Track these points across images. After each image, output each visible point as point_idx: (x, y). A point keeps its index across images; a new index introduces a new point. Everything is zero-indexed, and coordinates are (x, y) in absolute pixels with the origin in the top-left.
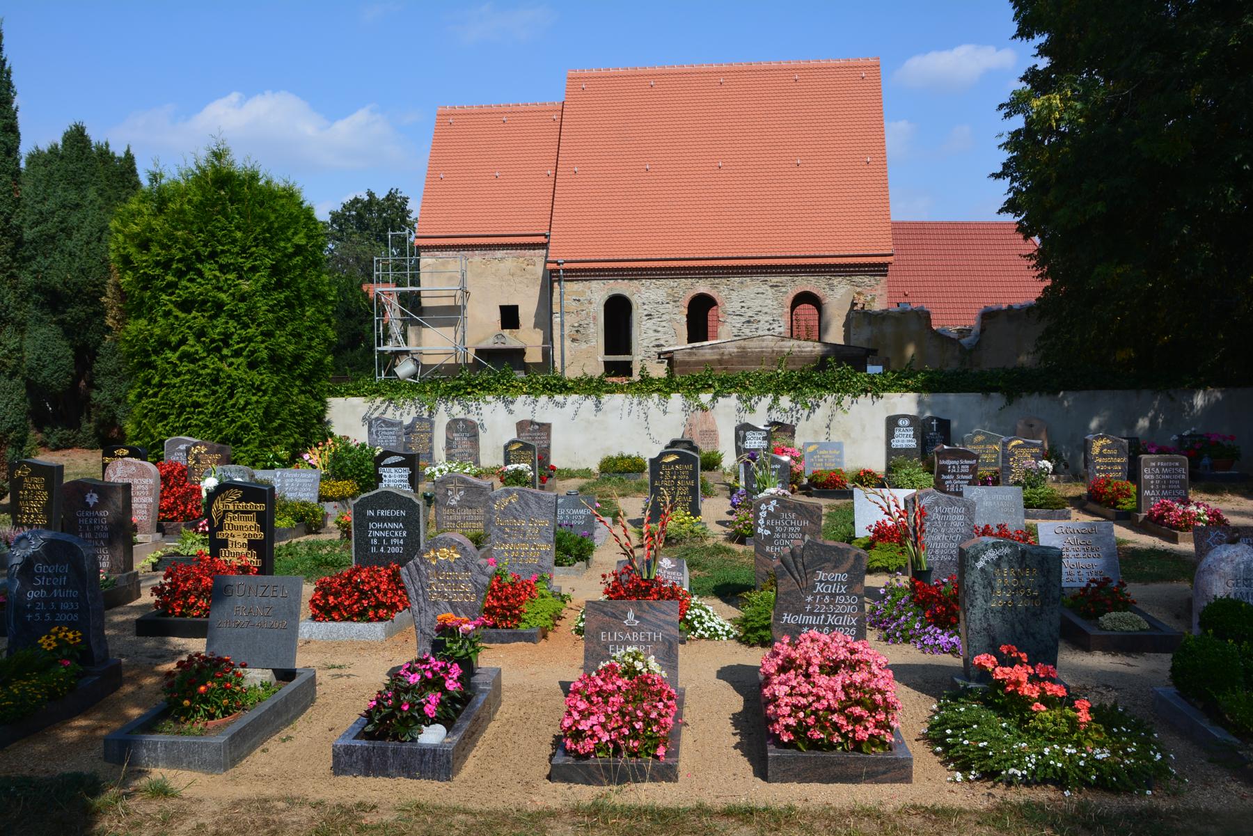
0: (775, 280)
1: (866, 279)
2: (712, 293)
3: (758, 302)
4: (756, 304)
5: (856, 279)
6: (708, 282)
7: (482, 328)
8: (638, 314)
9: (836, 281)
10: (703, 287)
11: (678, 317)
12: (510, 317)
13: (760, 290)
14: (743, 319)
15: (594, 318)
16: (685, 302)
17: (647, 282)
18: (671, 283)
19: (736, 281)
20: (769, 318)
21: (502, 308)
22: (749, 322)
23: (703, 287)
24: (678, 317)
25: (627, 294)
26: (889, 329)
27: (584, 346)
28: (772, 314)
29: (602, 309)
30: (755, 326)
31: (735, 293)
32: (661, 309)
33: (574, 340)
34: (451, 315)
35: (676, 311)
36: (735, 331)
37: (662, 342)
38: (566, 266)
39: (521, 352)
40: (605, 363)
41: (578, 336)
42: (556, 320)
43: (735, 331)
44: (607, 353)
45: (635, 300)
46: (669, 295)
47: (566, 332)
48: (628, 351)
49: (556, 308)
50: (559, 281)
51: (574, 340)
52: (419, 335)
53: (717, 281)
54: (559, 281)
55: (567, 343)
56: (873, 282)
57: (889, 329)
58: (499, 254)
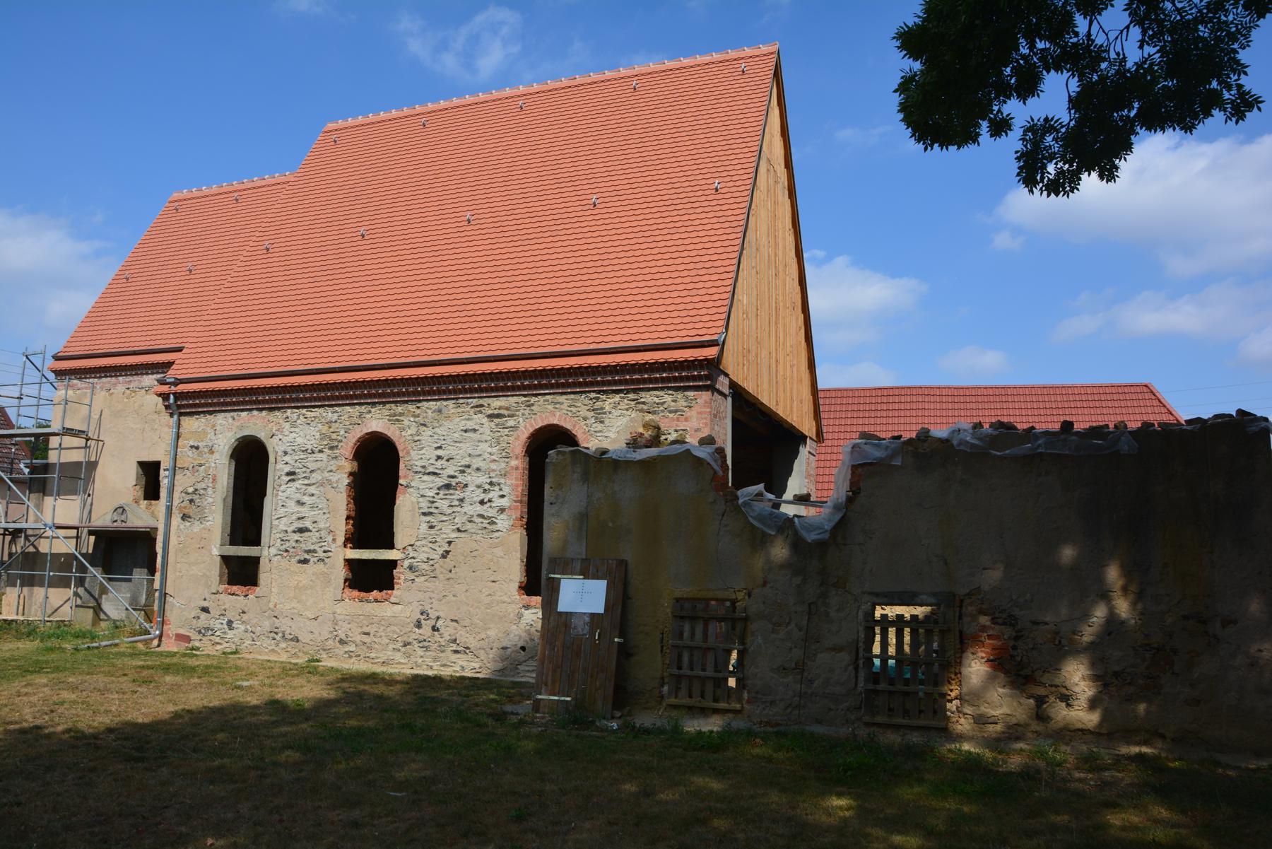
0: (497, 403)
1: (667, 398)
2: (391, 432)
3: (466, 448)
4: (460, 453)
5: (649, 397)
6: (386, 410)
7: (113, 497)
8: (276, 471)
9: (608, 402)
10: (376, 420)
11: (334, 477)
13: (470, 425)
14: (440, 482)
16: (347, 448)
18: (329, 414)
19: (429, 407)
20: (483, 479)
21: (141, 464)
22: (448, 486)
23: (376, 420)
24: (334, 477)
25: (262, 436)
26: (627, 490)
27: (197, 527)
30: (458, 494)
31: (427, 432)
33: (185, 517)
35: (333, 465)
36: (424, 504)
37: (308, 524)
38: (181, 388)
41: (191, 511)
43: (424, 504)
45: (274, 447)
46: (324, 436)
47: (176, 503)
48: (256, 541)
51: (185, 517)
53: (400, 409)
55: (176, 520)
56: (682, 403)
57: (627, 490)
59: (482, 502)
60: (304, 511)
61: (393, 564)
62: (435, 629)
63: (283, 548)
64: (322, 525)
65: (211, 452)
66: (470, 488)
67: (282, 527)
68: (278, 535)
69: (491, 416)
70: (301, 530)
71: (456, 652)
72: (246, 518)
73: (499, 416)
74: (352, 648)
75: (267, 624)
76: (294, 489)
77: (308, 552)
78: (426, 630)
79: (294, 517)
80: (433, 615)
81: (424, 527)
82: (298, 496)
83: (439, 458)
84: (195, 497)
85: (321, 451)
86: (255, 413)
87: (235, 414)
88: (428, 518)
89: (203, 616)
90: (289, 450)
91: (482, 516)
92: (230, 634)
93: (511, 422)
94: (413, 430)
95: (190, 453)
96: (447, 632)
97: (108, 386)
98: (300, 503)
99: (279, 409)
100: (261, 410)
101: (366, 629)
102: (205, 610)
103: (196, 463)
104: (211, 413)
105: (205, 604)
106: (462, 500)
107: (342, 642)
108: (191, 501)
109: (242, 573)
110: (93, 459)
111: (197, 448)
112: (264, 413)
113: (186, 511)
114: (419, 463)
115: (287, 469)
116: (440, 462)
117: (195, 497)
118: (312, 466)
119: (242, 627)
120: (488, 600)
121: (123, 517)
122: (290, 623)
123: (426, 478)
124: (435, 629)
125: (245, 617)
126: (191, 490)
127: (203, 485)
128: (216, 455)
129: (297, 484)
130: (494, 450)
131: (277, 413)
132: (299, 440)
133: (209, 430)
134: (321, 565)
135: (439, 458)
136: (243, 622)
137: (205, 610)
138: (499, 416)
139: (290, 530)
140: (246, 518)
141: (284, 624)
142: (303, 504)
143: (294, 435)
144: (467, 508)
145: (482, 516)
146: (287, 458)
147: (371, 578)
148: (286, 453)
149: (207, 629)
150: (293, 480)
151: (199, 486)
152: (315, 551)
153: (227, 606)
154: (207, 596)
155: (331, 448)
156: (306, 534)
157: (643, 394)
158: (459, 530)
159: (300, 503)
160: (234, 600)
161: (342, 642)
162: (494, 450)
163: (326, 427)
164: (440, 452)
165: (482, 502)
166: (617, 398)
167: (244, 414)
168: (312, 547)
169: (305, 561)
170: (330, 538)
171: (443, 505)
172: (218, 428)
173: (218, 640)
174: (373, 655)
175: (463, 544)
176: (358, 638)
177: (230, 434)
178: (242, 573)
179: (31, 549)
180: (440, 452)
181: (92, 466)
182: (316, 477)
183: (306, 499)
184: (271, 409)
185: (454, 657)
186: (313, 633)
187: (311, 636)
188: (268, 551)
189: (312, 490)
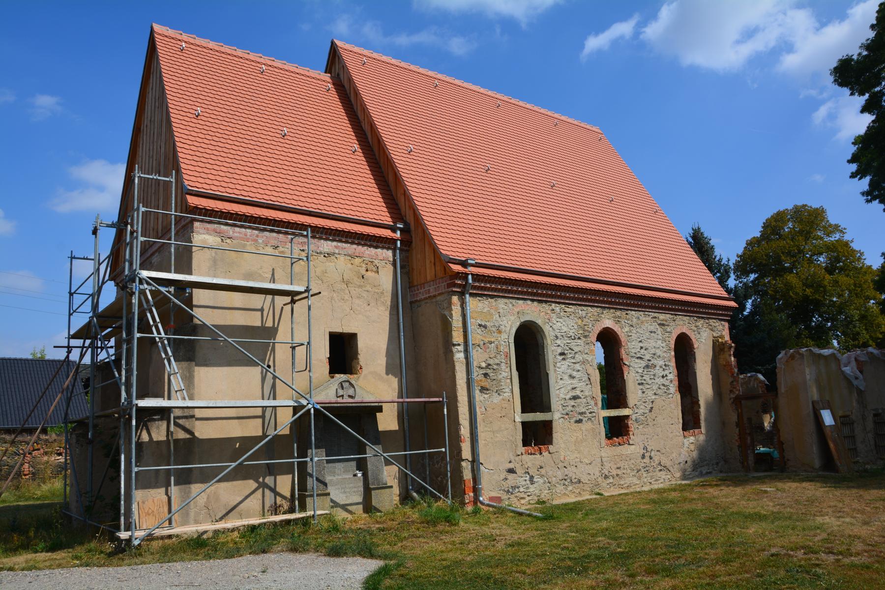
2: (616, 328)
8: (552, 351)
9: (700, 323)
10: (608, 321)
12: (343, 353)
15: (507, 356)
17: (557, 308)
18: (581, 311)
20: (661, 363)
23: (608, 321)
25: (539, 322)
27: (496, 399)
28: (664, 358)
29: (512, 340)
30: (653, 371)
32: (573, 344)
33: (483, 389)
34: (251, 346)
37: (578, 393)
39: (371, 411)
40: (524, 424)
42: (459, 356)
44: (524, 411)
48: (547, 408)
49: (457, 337)
50: (462, 295)
52: (189, 380)
53: (618, 313)
54: (462, 295)
56: (721, 327)
58: (327, 246)
59: (663, 377)
60: (575, 381)
61: (627, 417)
62: (651, 458)
63: (564, 412)
64: (587, 393)
65: (500, 332)
66: (658, 368)
67: (562, 396)
68: (560, 402)
69: (659, 324)
70: (575, 398)
71: (661, 470)
72: (534, 390)
73: (663, 325)
74: (611, 480)
75: (560, 474)
76: (566, 366)
77: (581, 414)
78: (647, 460)
79: (569, 388)
80: (649, 450)
81: (640, 392)
82: (570, 371)
83: (642, 348)
84: (488, 371)
85: (579, 338)
86: (529, 302)
87: (514, 301)
88: (641, 387)
89: (511, 476)
90: (559, 335)
91: (663, 385)
92: (532, 489)
93: (669, 330)
94: (627, 329)
95: (479, 331)
96: (656, 459)
97: (274, 242)
98: (572, 377)
99: (546, 302)
100: (533, 300)
101: (618, 465)
102: (511, 471)
103: (486, 340)
104: (492, 297)
105: (511, 466)
106: (654, 375)
107: (606, 477)
108: (486, 375)
109: (537, 435)
110: (269, 324)
111: (485, 327)
112: (536, 303)
113: (483, 384)
114: (633, 351)
115: (559, 350)
116: (642, 351)
117: (488, 371)
118: (576, 349)
119: (541, 481)
120: (671, 435)
121: (351, 392)
122: (574, 468)
123: (637, 360)
124: (651, 458)
125: (543, 471)
126: (484, 365)
127: (497, 361)
128: (504, 336)
129: (566, 363)
130: (664, 345)
131: (544, 305)
132: (565, 329)
133: (492, 311)
134: (590, 423)
135: (642, 348)
136: (542, 476)
137: (511, 471)
138: (663, 325)
139: (568, 397)
140: (534, 390)
141: (571, 472)
142: (574, 377)
143: (559, 324)
144: (657, 380)
145: (663, 385)
146: (558, 342)
147: (617, 429)
148: (557, 337)
149: (514, 488)
150: (564, 359)
151: (491, 362)
152: (585, 413)
153: (529, 464)
154: (512, 458)
155: (585, 337)
156: (578, 401)
157: (711, 321)
158: (655, 394)
159: (572, 377)
160: (532, 460)
161: (606, 477)
162: (664, 345)
163: (580, 321)
164: (641, 344)
165: (663, 377)
166: (702, 321)
167: (521, 302)
168: (583, 410)
169: (579, 421)
170: (592, 403)
171: (647, 377)
172: (501, 311)
173: (522, 495)
174: (622, 483)
175: (659, 401)
176: (614, 472)
177: (512, 318)
178: (537, 435)
179: (181, 435)
180: (641, 344)
181: (271, 332)
182: (579, 357)
183: (575, 374)
184: (540, 301)
185: (659, 474)
186: (588, 473)
187: (589, 477)
188: (556, 416)
189: (577, 367)
